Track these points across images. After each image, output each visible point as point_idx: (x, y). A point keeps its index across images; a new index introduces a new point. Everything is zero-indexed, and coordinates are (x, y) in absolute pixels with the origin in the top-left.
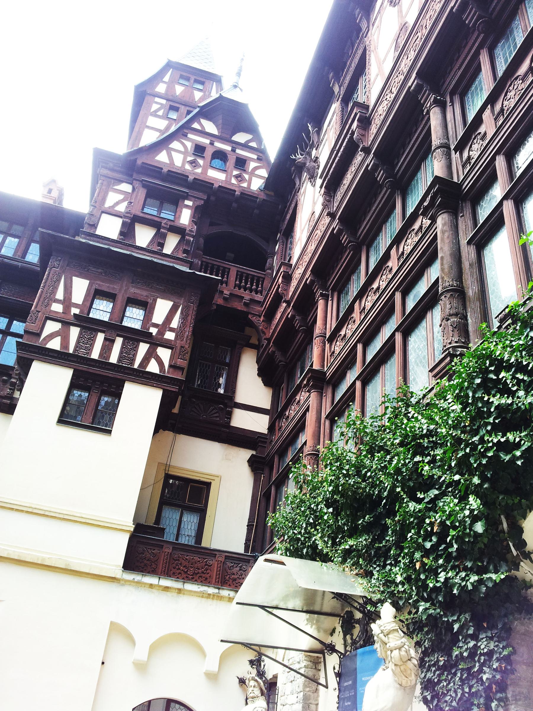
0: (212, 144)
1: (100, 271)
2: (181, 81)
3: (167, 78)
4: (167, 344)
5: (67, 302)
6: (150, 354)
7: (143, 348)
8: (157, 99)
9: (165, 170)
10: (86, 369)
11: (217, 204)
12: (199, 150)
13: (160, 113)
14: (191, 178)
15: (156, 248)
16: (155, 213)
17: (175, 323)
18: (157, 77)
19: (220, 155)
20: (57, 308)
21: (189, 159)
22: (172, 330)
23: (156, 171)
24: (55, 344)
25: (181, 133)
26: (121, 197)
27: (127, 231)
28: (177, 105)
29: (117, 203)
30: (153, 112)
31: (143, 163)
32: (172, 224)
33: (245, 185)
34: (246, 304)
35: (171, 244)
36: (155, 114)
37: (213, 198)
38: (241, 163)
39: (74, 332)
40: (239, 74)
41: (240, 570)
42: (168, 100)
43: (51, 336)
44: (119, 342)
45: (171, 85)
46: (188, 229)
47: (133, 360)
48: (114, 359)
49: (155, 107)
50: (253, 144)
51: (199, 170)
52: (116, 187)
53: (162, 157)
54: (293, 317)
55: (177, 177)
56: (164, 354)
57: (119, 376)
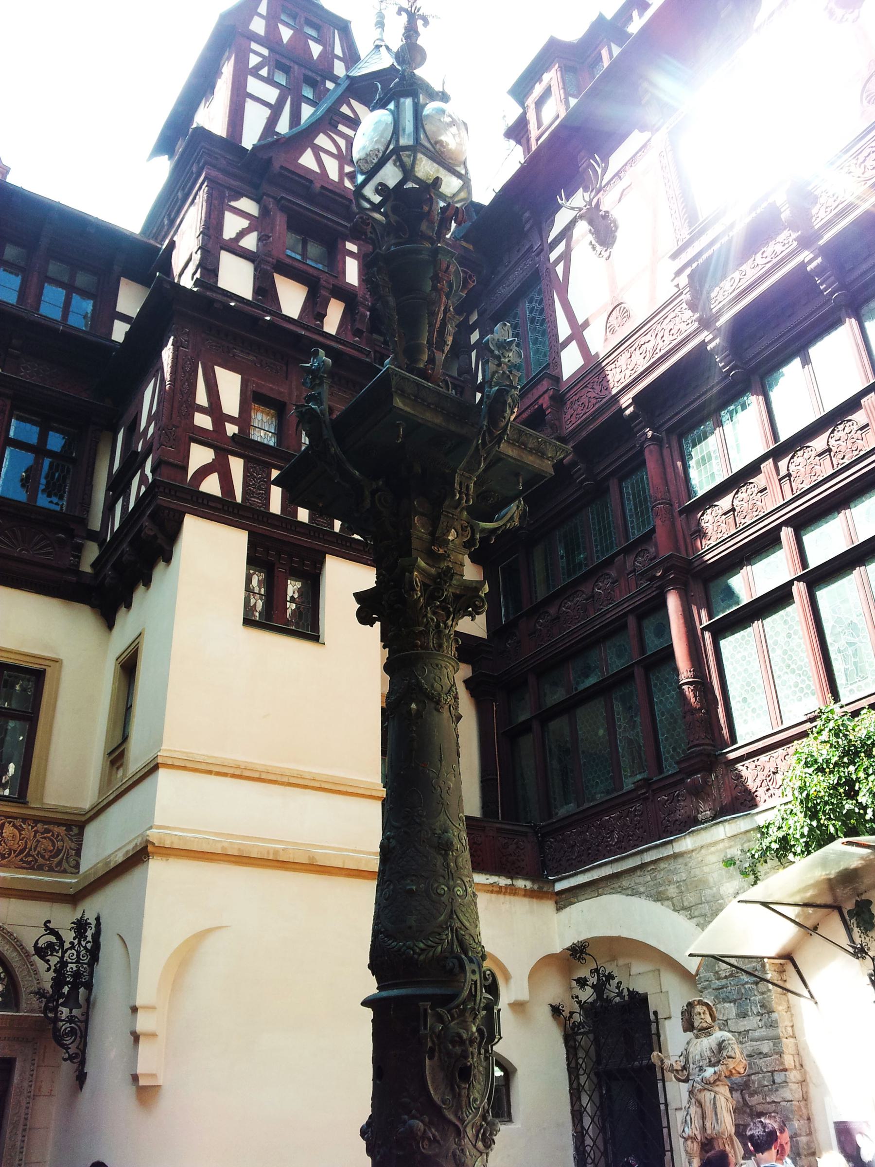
1: (251, 358)
2: (283, 17)
5: (214, 409)
8: (254, 46)
9: (317, 185)
10: (268, 533)
15: (313, 323)
16: (299, 257)
20: (203, 421)
27: (265, 289)
28: (288, 62)
29: (242, 234)
30: (253, 68)
31: (282, 167)
32: (335, 282)
35: (333, 318)
39: (237, 466)
41: (518, 847)
43: (204, 472)
49: (254, 60)
57: (317, 544)
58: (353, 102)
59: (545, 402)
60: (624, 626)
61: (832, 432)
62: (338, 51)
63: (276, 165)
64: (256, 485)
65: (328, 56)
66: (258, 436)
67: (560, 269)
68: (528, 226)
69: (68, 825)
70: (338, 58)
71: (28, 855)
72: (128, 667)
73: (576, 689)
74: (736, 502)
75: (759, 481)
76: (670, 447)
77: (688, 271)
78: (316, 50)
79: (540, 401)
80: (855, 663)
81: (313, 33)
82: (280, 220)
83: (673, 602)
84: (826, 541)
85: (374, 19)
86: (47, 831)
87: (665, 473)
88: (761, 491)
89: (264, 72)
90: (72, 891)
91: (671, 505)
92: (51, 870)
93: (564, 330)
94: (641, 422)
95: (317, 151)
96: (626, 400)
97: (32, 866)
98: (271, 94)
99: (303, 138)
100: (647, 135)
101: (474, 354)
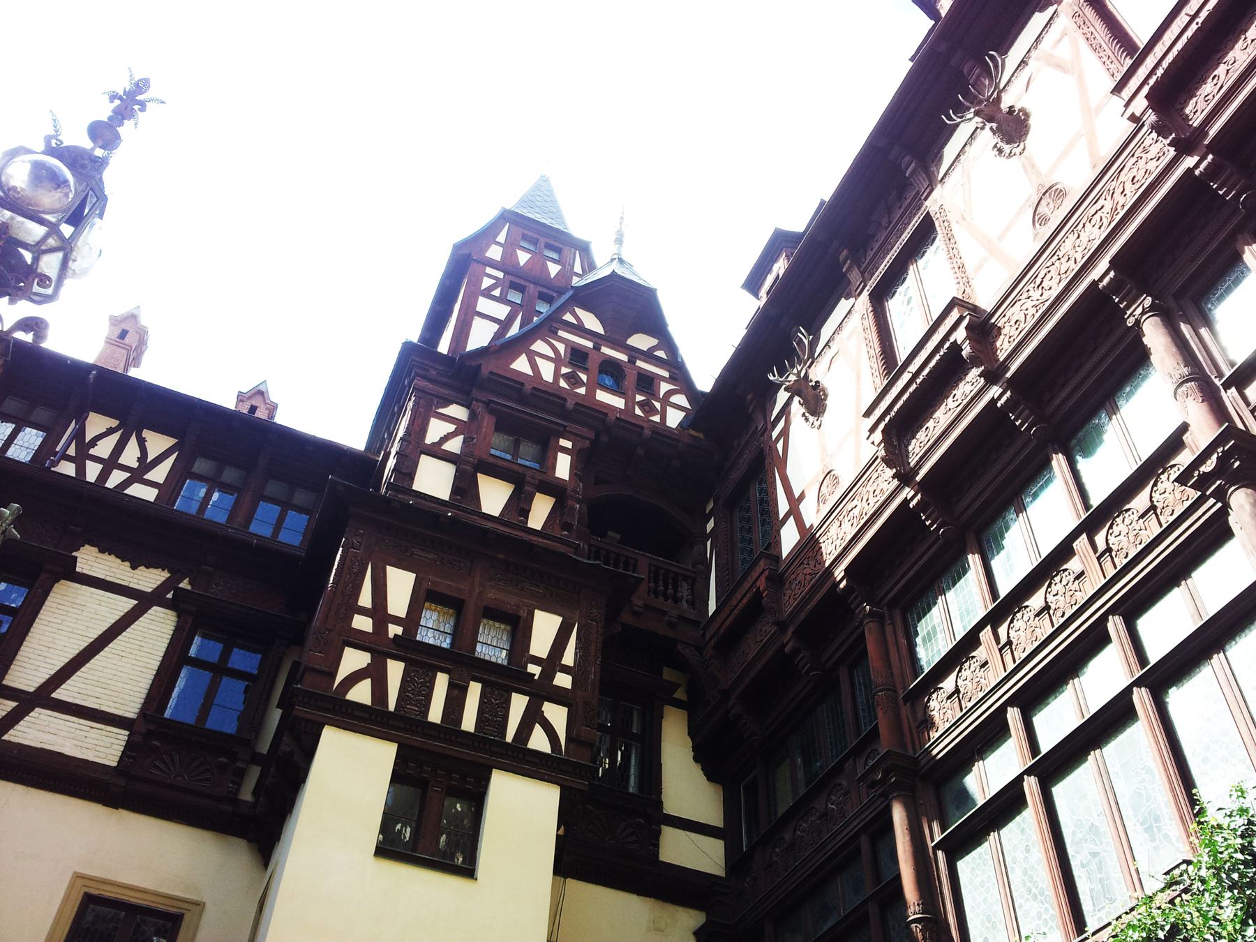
0: (597, 348)
1: (431, 556)
2: (523, 244)
3: (501, 238)
4: (559, 697)
5: (379, 611)
6: (533, 716)
7: (518, 704)
8: (489, 270)
9: (528, 387)
11: (616, 449)
12: (577, 357)
13: (497, 293)
14: (570, 404)
15: (516, 519)
16: (509, 457)
17: (569, 658)
18: (486, 235)
19: (610, 367)
20: (362, 623)
21: (564, 370)
22: (566, 669)
23: (516, 387)
24: (361, 693)
25: (549, 328)
26: (451, 428)
27: (465, 488)
28: (523, 283)
32: (543, 477)
33: (657, 419)
34: (671, 625)
35: (540, 511)
36: (487, 294)
37: (604, 438)
38: (647, 383)
39: (395, 671)
40: (619, 241)
42: (505, 273)
44: (475, 690)
45: (510, 248)
46: (569, 489)
48: (469, 722)
49: (486, 282)
50: (661, 354)
51: (582, 391)
52: (441, 411)
53: (521, 365)
54: (796, 651)
56: (557, 715)
57: (483, 757)
58: (577, 310)
59: (762, 583)
60: (858, 851)
61: (1049, 586)
63: (485, 372)
64: (417, 691)
65: (567, 273)
66: (427, 636)
67: (780, 446)
68: (751, 408)
74: (960, 683)
75: (980, 653)
76: (893, 624)
77: (882, 426)
78: (554, 269)
79: (758, 584)
80: (1101, 880)
81: (555, 256)
82: (488, 422)
83: (899, 815)
84: (1057, 721)
85: (614, 237)
87: (887, 655)
88: (982, 666)
89: (497, 293)
91: (895, 692)
93: (783, 506)
94: (856, 598)
95: (532, 357)
96: (839, 573)
99: (521, 344)
100: (852, 300)
101: (709, 543)
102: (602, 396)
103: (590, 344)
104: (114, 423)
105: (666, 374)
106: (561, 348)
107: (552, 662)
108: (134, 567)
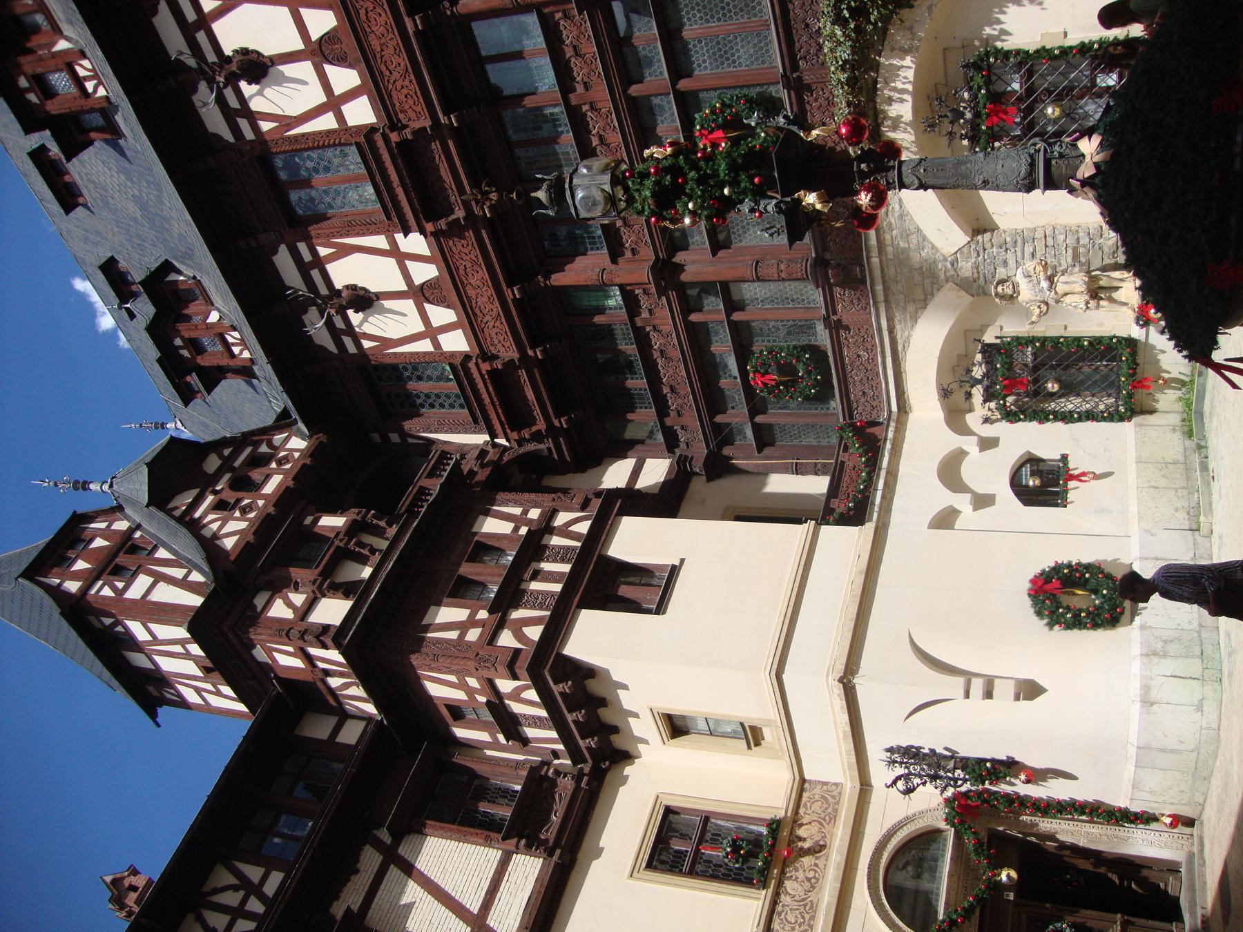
5: (463, 627)
6: (564, 531)
9: (251, 538)
14: (271, 510)
17: (517, 511)
20: (473, 635)
21: (237, 514)
24: (534, 633)
29: (289, 604)
33: (297, 455)
42: (97, 578)
46: (354, 517)
47: (568, 548)
50: (227, 452)
55: (264, 528)
59: (485, 367)
62: (103, 525)
69: (801, 791)
70: (109, 527)
71: (824, 819)
72: (676, 727)
73: (735, 378)
78: (99, 542)
86: (805, 806)
90: (858, 786)
92: (838, 803)
93: (425, 346)
97: (833, 818)
98: (143, 581)
102: (270, 488)
103: (210, 499)
104: (190, 918)
105: (249, 450)
106: (211, 517)
107: (517, 521)
108: (357, 871)
